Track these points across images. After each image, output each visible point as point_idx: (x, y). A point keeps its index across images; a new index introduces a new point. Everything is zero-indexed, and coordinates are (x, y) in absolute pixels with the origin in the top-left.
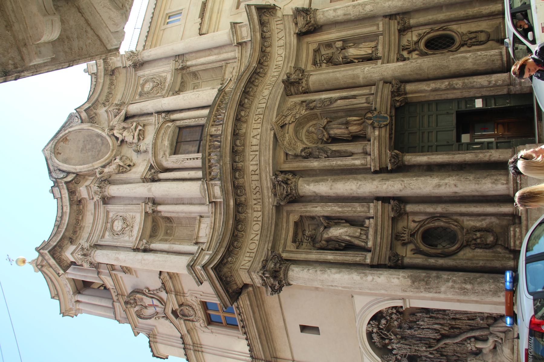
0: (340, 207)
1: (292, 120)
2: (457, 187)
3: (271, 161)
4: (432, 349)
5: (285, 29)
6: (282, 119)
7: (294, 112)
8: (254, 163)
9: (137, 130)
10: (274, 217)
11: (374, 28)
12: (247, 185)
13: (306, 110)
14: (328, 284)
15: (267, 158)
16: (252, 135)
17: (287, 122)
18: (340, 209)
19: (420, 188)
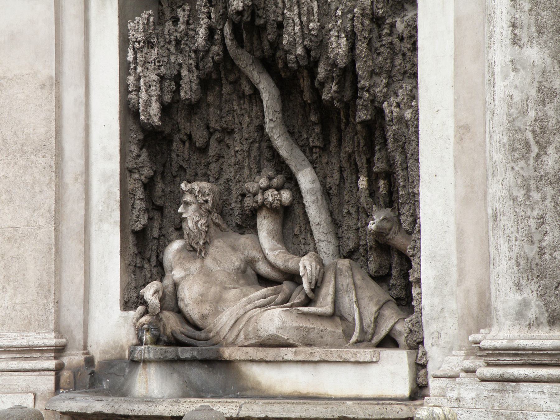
4: (228, 41)
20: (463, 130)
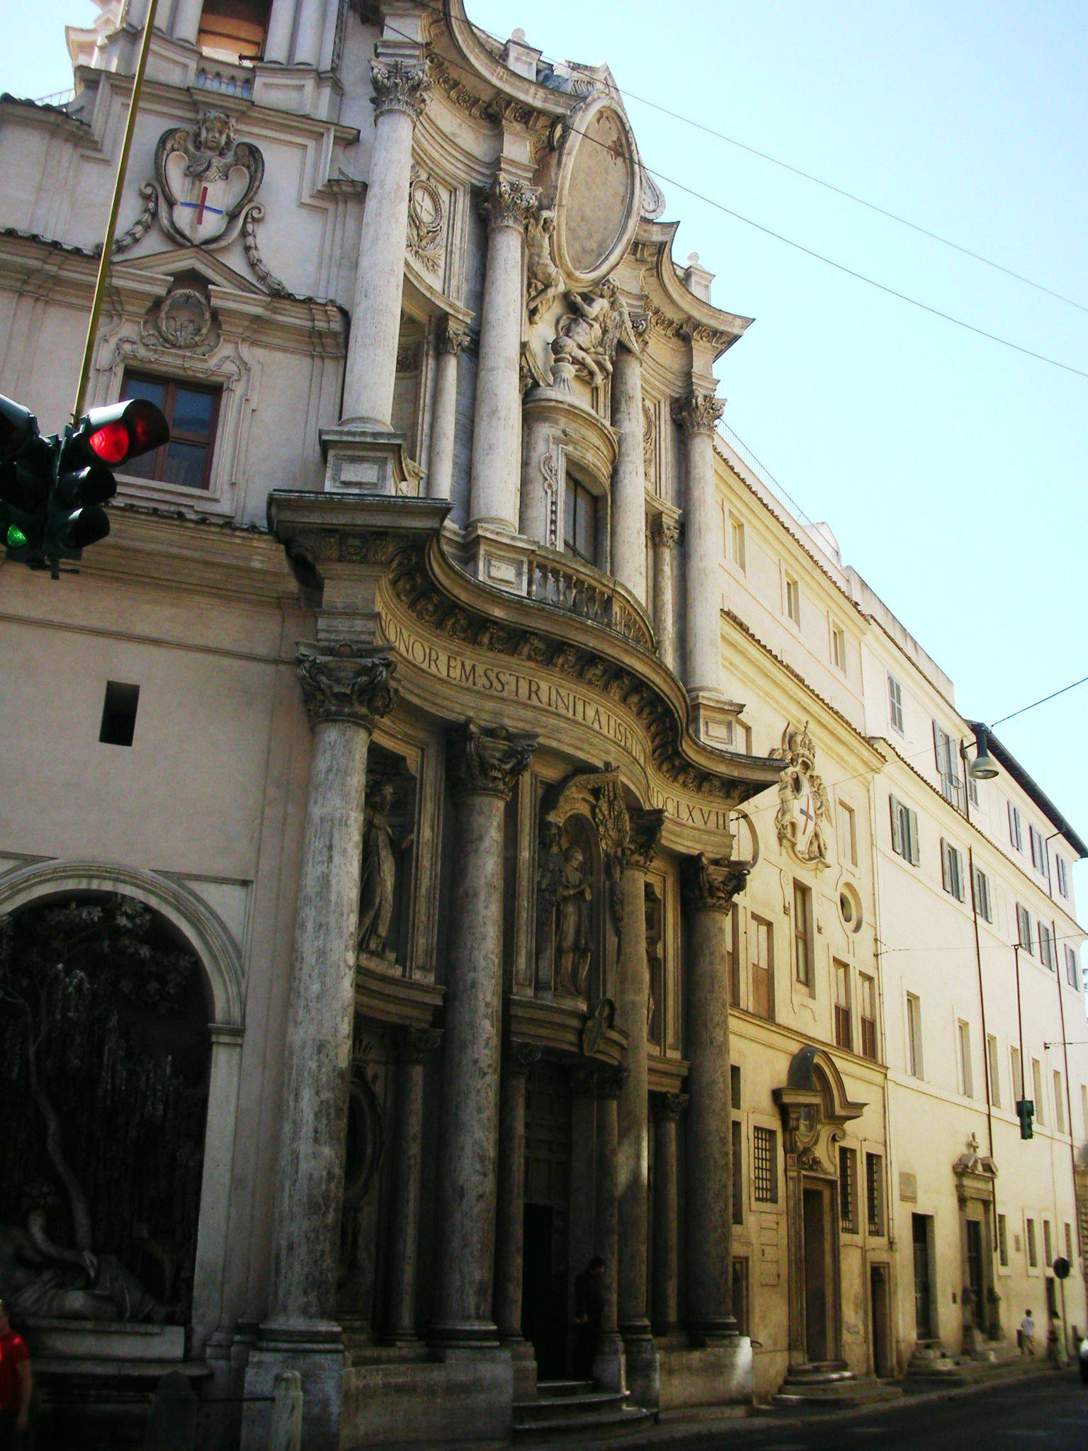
0: (428, 890)
1: (600, 816)
2: (478, 1200)
3: (554, 744)
5: (706, 832)
6: (611, 794)
7: (610, 825)
8: (554, 697)
9: (595, 368)
10: (433, 710)
11: (670, 1039)
12: (514, 661)
13: (607, 855)
14: (336, 836)
15: (563, 737)
16: (601, 709)
17: (601, 802)
18: (423, 890)
19: (479, 1111)
20: (237, 1182)
